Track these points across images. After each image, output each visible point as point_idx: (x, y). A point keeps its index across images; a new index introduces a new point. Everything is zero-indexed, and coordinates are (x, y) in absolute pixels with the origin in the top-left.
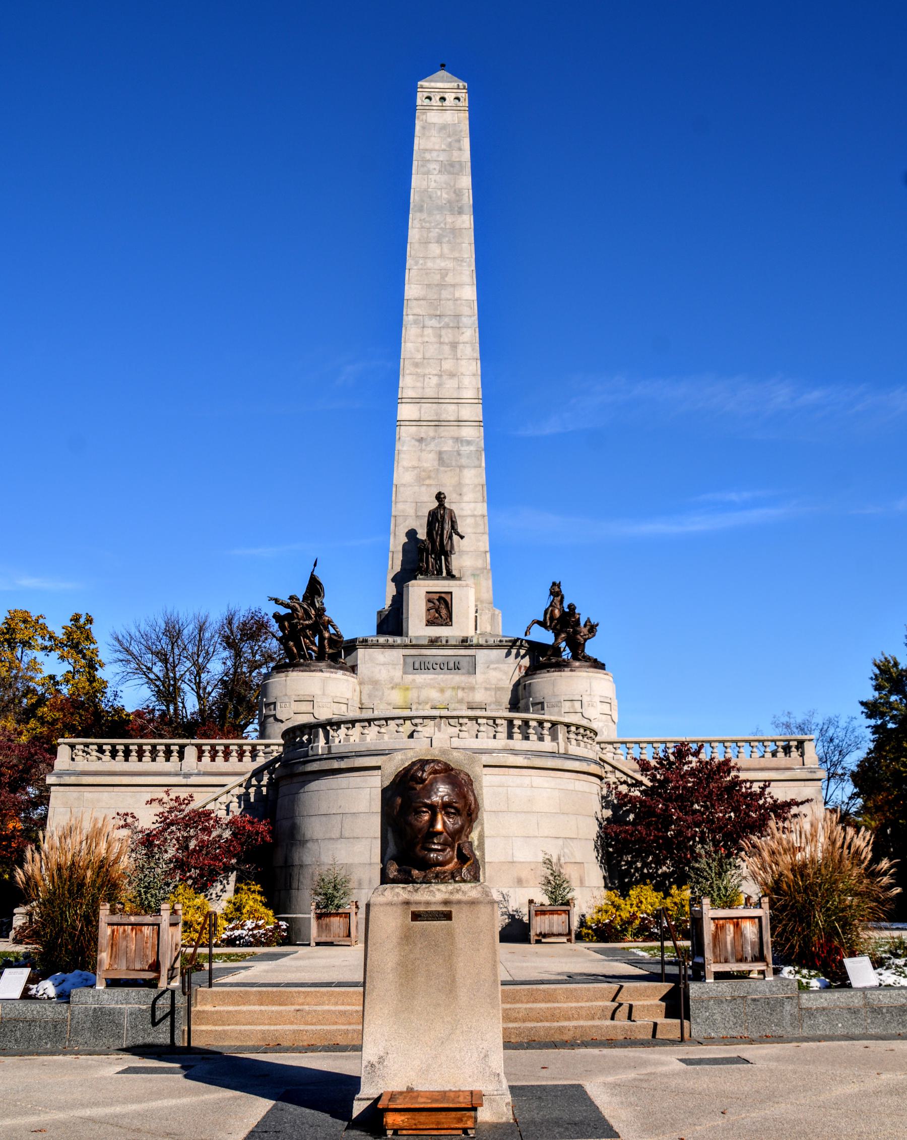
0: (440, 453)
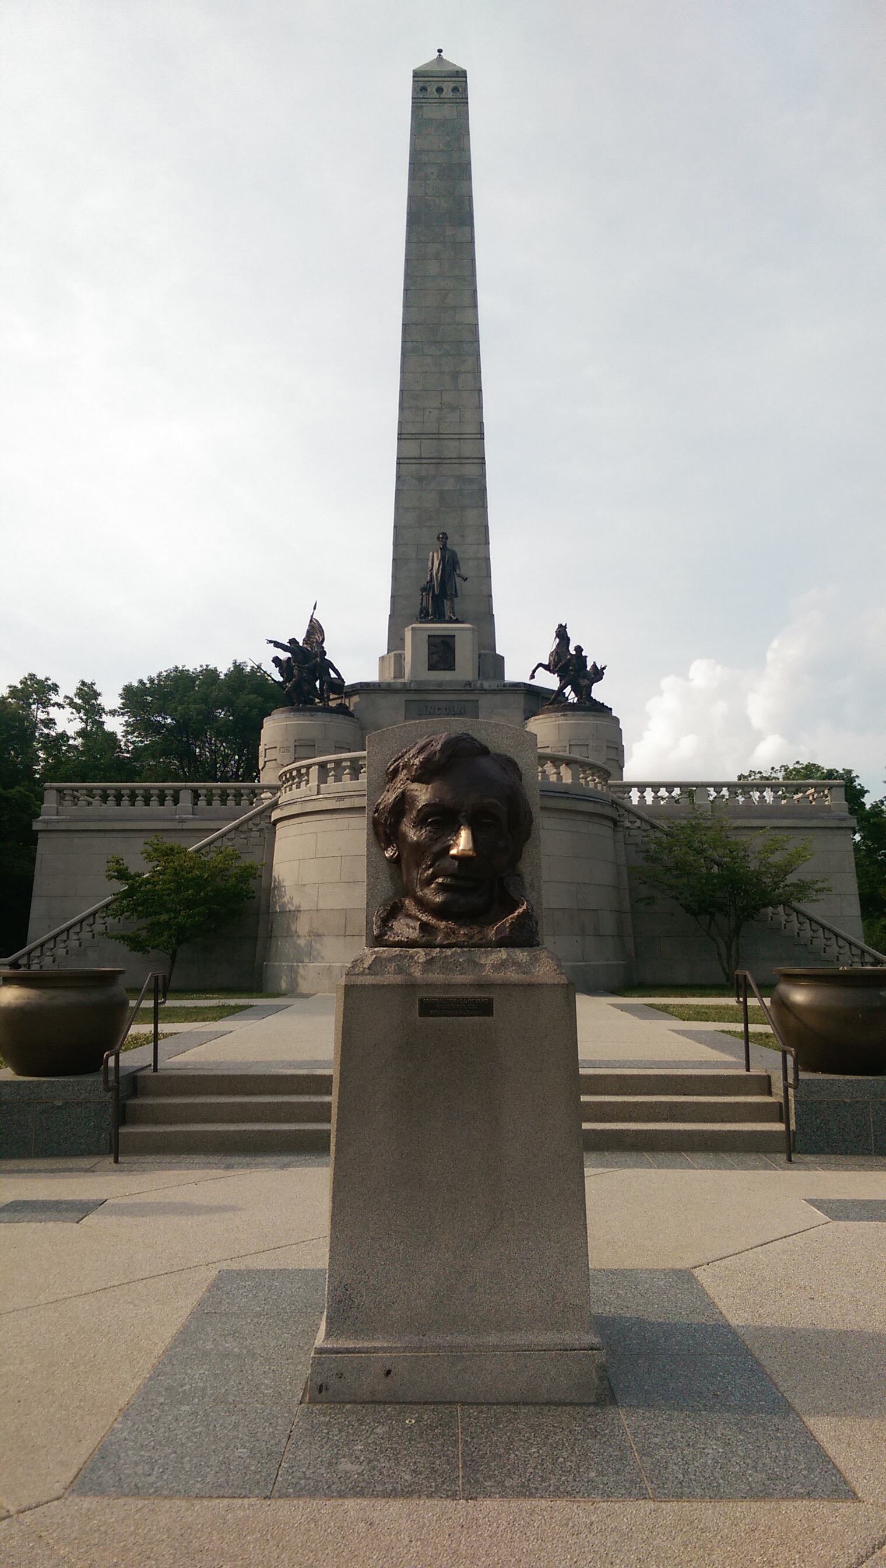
0: (442, 494)
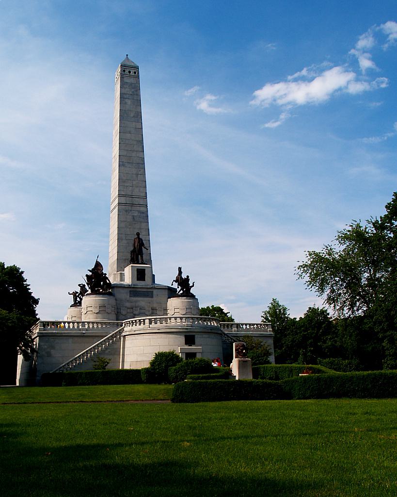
0: (133, 216)
